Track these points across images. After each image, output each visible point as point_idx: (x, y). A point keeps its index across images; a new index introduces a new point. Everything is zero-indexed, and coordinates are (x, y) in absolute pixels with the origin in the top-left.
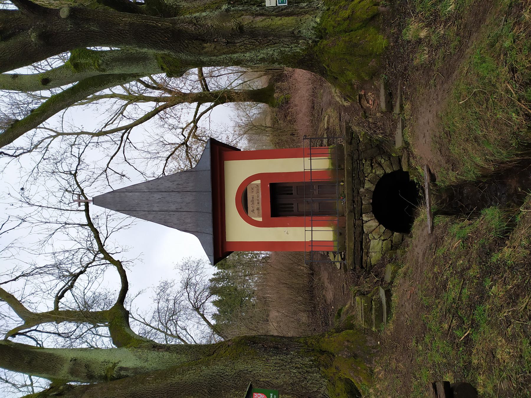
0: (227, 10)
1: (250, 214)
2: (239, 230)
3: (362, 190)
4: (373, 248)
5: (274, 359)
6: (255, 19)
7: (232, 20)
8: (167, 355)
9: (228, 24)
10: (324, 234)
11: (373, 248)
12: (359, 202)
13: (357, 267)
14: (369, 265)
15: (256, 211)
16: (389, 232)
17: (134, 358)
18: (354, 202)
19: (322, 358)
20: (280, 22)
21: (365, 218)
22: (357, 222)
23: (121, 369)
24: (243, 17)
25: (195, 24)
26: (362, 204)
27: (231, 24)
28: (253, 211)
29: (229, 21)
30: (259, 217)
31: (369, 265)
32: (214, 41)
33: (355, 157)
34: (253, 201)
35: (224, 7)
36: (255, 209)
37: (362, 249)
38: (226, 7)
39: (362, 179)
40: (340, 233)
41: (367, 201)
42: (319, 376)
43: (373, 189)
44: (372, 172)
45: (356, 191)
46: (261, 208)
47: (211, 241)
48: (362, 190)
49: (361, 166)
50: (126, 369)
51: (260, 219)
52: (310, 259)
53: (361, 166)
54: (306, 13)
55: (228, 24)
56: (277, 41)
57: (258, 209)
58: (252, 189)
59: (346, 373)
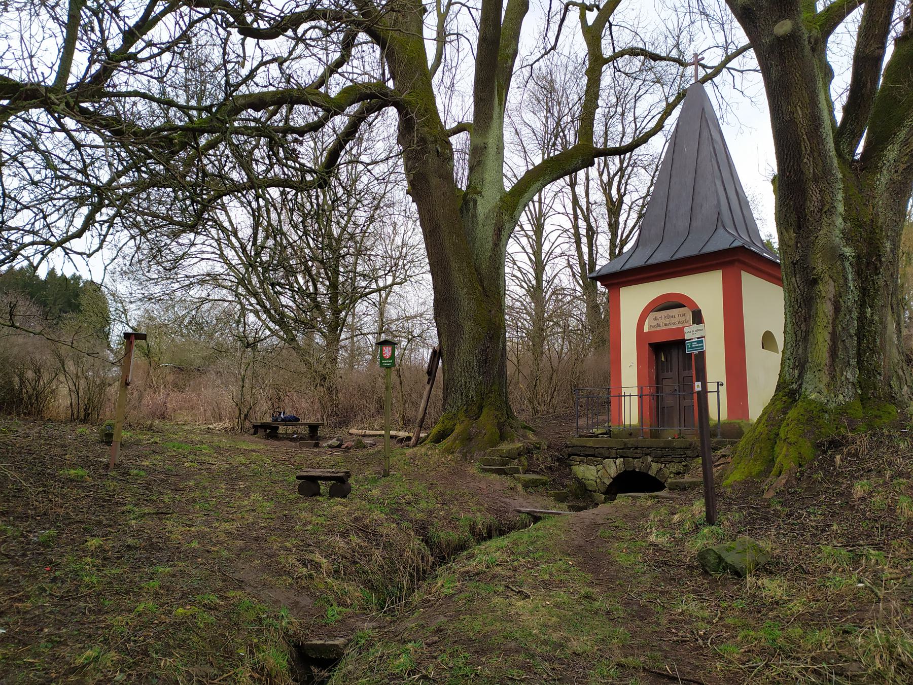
0: (842, 257)
1: (652, 315)
2: (634, 301)
3: (649, 459)
4: (588, 469)
5: (473, 359)
6: (828, 301)
7: (825, 267)
8: (489, 246)
9: (819, 261)
10: (631, 413)
11: (588, 469)
12: (638, 455)
13: (570, 449)
14: (572, 463)
15: (655, 323)
16: (603, 489)
17: (487, 211)
18: (636, 448)
19: (475, 408)
20: (821, 340)
21: (619, 461)
22: (614, 451)
23: (475, 201)
24: (831, 282)
25: (821, 210)
26: (635, 458)
27: (820, 265)
28: (656, 319)
29: (823, 262)
30: (650, 327)
31: (572, 463)
32: (797, 243)
33: (689, 452)
34: (667, 317)
35: (848, 251)
36: (657, 322)
37: (587, 456)
38: (848, 254)
39: (662, 460)
40: (631, 432)
41: (637, 464)
42: (459, 404)
43: (650, 473)
44: (671, 473)
45: (648, 451)
46: (659, 329)
47: (614, 270)
48: (649, 459)
49: (678, 460)
50: (475, 206)
51: (646, 330)
52: (605, 398)
53: (678, 460)
54: (833, 378)
55: (819, 261)
56: (799, 338)
57: (658, 325)
58: (684, 315)
59: (458, 428)
